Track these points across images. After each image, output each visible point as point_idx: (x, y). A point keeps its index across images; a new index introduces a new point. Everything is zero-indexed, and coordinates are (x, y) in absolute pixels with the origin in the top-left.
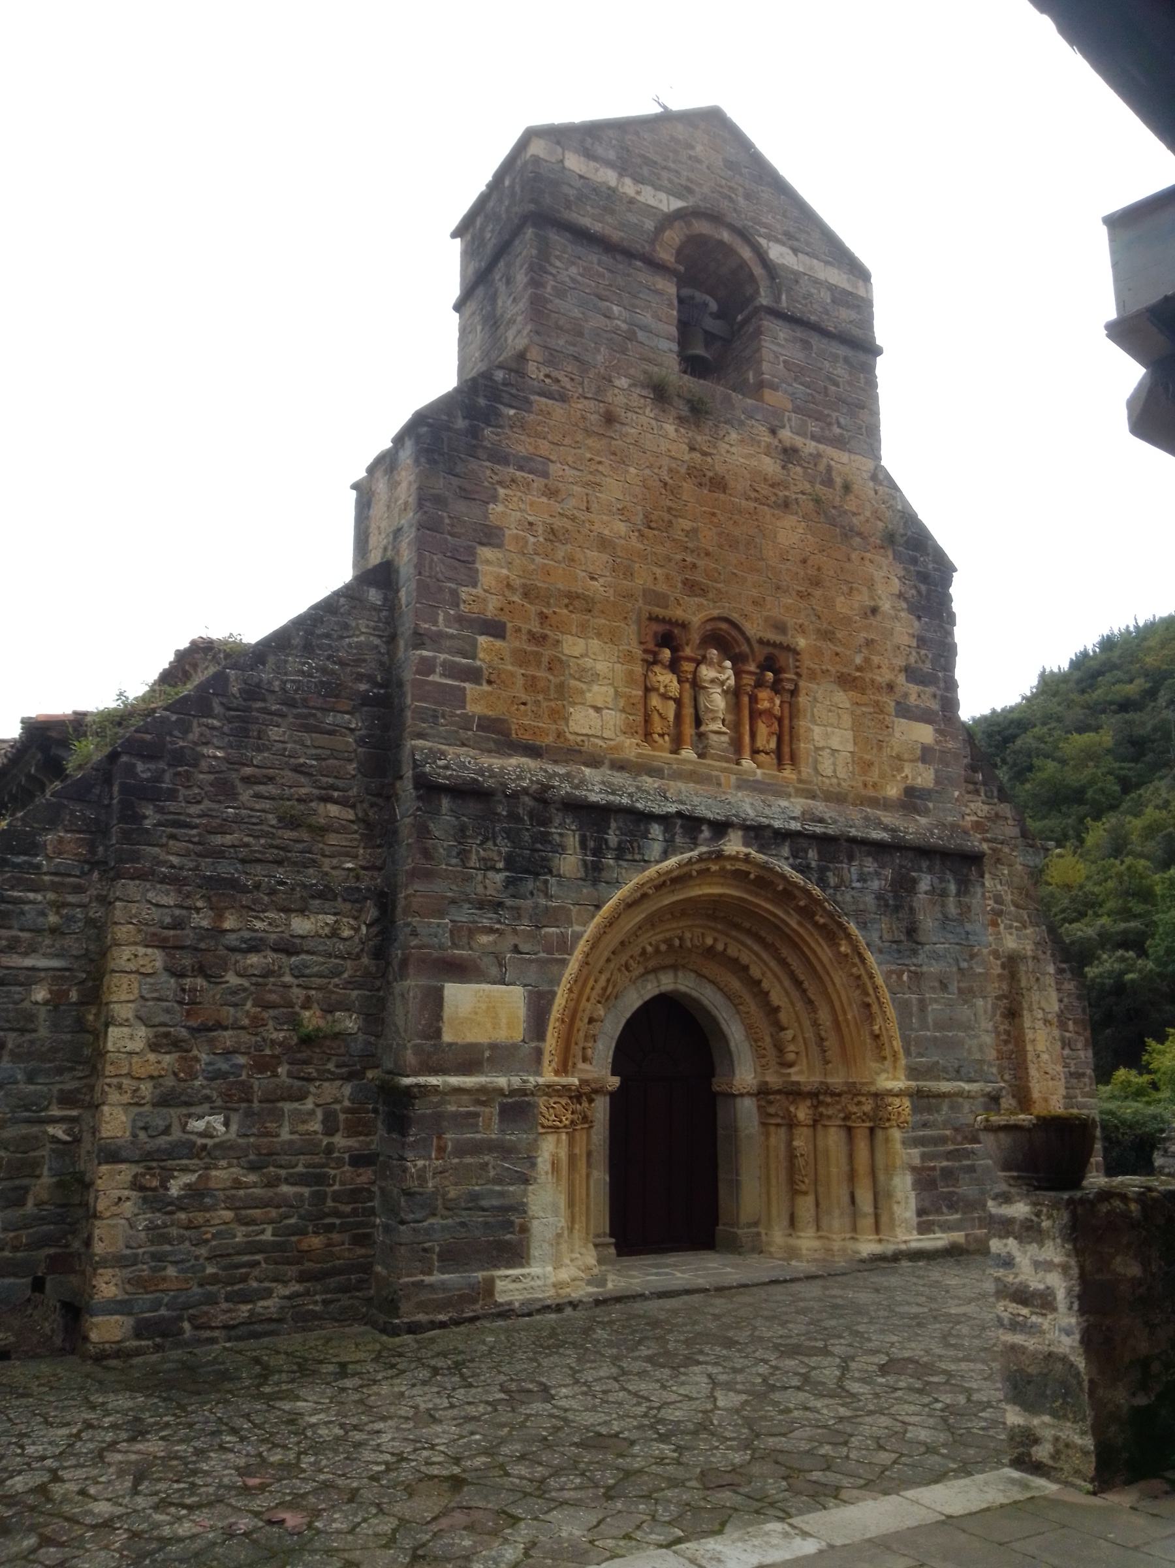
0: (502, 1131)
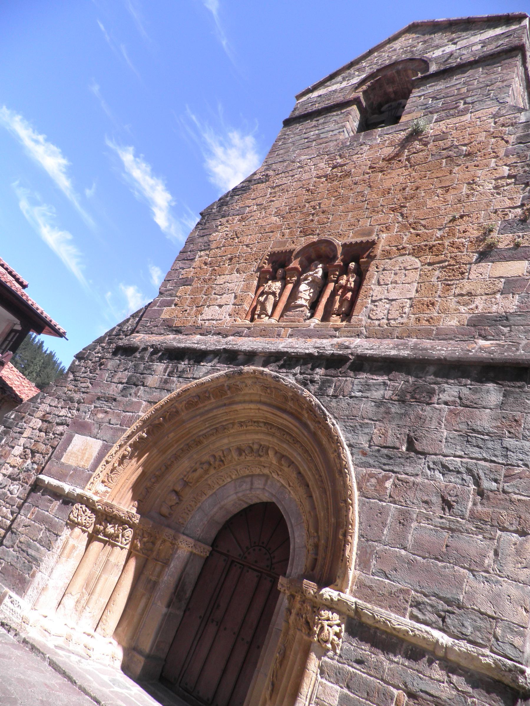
0: (55, 516)
